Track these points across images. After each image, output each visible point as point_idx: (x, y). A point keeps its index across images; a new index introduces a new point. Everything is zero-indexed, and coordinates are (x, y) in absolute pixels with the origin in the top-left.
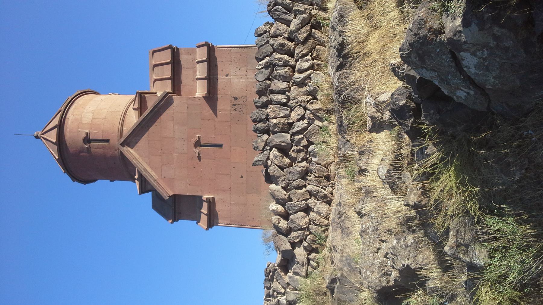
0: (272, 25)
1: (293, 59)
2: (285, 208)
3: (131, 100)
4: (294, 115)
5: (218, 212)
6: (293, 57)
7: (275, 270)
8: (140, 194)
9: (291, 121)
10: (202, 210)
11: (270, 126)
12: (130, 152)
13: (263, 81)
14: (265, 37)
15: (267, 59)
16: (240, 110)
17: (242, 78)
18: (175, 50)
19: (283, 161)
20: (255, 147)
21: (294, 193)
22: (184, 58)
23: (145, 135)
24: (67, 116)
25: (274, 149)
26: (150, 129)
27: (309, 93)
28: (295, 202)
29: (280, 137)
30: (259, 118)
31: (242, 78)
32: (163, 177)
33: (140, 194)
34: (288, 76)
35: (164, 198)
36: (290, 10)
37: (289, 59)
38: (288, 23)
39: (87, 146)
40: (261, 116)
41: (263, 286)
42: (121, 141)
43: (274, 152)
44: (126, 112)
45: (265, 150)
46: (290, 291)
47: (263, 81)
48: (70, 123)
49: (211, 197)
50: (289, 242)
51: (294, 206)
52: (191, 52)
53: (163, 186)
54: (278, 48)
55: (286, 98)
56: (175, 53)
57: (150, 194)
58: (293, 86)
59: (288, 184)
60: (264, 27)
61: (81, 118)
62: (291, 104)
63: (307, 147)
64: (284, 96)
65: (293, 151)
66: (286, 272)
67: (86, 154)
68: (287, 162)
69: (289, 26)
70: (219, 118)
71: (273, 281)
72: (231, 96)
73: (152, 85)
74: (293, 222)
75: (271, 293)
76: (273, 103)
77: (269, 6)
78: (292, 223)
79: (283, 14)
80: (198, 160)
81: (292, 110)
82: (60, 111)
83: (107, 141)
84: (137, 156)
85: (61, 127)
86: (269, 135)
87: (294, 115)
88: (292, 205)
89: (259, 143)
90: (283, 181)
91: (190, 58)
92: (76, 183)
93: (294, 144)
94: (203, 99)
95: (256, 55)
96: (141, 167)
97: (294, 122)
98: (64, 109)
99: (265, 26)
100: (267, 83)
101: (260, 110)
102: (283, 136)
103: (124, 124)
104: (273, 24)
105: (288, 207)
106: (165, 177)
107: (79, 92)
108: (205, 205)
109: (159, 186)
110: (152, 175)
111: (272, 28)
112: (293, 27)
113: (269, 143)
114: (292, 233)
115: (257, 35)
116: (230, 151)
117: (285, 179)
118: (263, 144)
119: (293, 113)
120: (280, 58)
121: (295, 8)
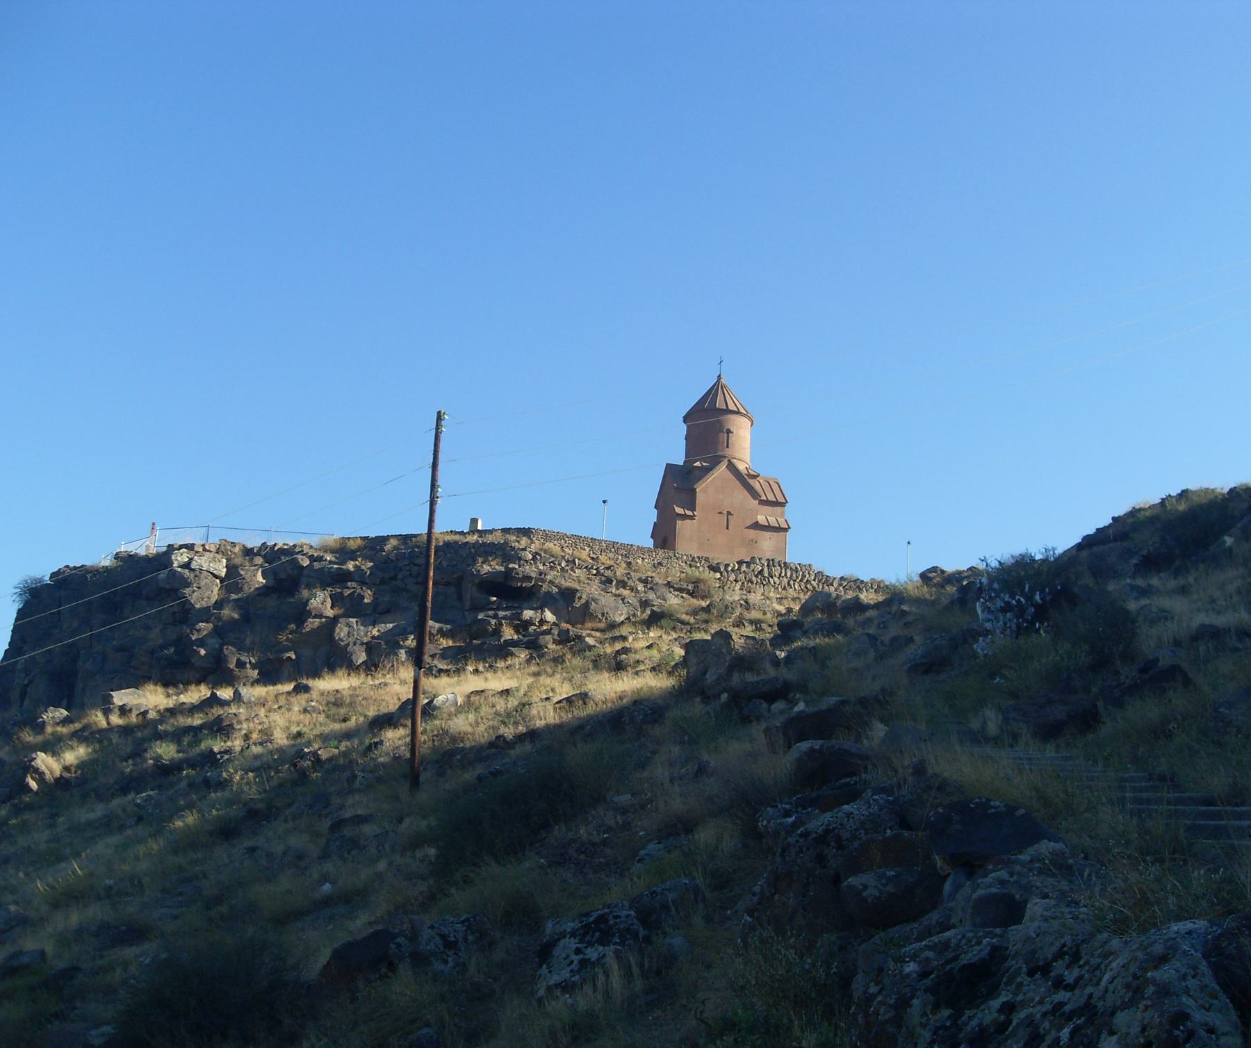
4: (776, 579)
6: (800, 581)
7: (709, 562)
22: (779, 508)
27: (785, 587)
36: (819, 582)
38: (814, 580)
39: (725, 430)
52: (782, 515)
56: (782, 505)
61: (741, 428)
63: (762, 583)
81: (779, 578)
83: (728, 447)
85: (738, 413)
108: (691, 514)
112: (813, 582)
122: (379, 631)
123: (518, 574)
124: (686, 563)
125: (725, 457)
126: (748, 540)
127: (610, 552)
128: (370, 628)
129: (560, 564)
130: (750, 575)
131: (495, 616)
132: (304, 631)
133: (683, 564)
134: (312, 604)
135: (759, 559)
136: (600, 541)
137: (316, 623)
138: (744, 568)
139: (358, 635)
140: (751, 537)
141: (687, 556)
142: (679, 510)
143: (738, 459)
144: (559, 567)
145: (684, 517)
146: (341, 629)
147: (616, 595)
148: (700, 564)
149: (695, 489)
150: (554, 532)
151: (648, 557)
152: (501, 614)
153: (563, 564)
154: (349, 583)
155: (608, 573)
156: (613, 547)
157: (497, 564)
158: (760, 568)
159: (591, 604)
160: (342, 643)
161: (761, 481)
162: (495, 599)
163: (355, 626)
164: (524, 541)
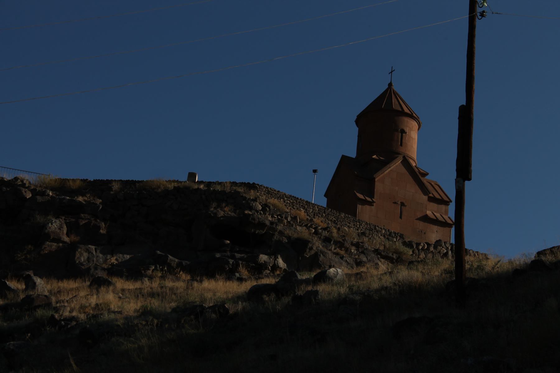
5: (365, 206)
7: (403, 239)
12: (399, 161)
13: (470, 253)
18: (448, 204)
22: (443, 207)
23: (408, 173)
24: (414, 121)
26: (411, 177)
39: (399, 130)
44: (414, 161)
48: (412, 122)
74: (422, 252)
82: (419, 118)
83: (401, 145)
85: (411, 116)
106: (385, 178)
118: (447, 246)
122: (116, 260)
123: (254, 219)
124: (384, 236)
125: (399, 154)
127: (322, 216)
128: (109, 256)
129: (286, 218)
131: (233, 257)
132: (42, 252)
133: (383, 237)
134: (50, 228)
135: (445, 243)
136: (314, 205)
137: (53, 247)
138: (432, 249)
139: (97, 261)
141: (385, 230)
142: (361, 196)
143: (410, 158)
144: (285, 221)
145: (365, 202)
146: (81, 254)
147: (334, 253)
148: (396, 240)
149: (374, 178)
150: (275, 191)
151: (353, 226)
152: (238, 255)
153: (289, 219)
154: (82, 215)
155: (325, 233)
156: (325, 212)
157: (229, 211)
158: (445, 251)
159: (320, 255)
160: (83, 267)
161: (425, 181)
162: (229, 242)
163: (94, 253)
164: (252, 194)
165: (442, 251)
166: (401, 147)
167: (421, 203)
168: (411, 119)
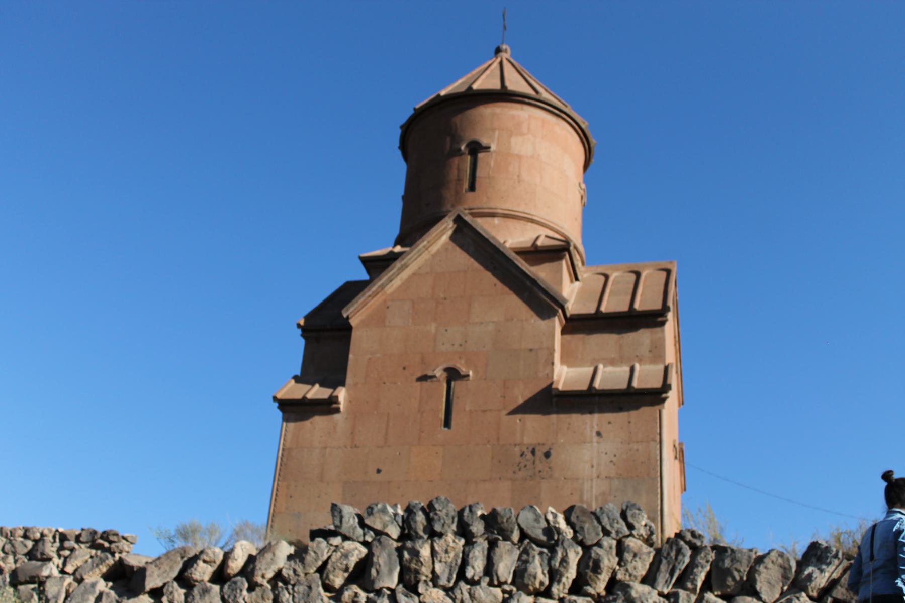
0: (648, 541)
1: (566, 591)
2: (236, 575)
3: (563, 231)
5: (311, 420)
7: (113, 554)
8: (360, 258)
9: (421, 588)
10: (317, 386)
11: (414, 542)
12: (442, 236)
13: (519, 525)
14: (619, 526)
15: (568, 532)
16: (522, 465)
17: (593, 467)
18: (660, 319)
19: (337, 571)
20: (372, 508)
21: (265, 597)
22: (644, 336)
23: (476, 265)
25: (364, 551)
26: (488, 275)
28: (244, 599)
29: (390, 563)
30: (436, 517)
31: (593, 467)
32: (389, 303)
33: (360, 258)
34: (526, 581)
35: (345, 309)
37: (566, 584)
38: (649, 579)
39: (463, 147)
40: (439, 520)
41: (86, 527)
42: (465, 215)
43: (357, 552)
45: (366, 530)
46: (66, 584)
47: (519, 525)
49: (342, 406)
50: (165, 585)
51: (235, 597)
53: (369, 304)
54: (590, 557)
55: (476, 578)
57: (365, 276)
58: (504, 592)
59: (286, 582)
60: (643, 523)
61: (522, 134)
62: (460, 589)
64: (480, 572)
65: (356, 595)
66: (106, 577)
67: (448, 147)
68: (334, 581)
69: (644, 581)
70: (506, 419)
71: (92, 547)
72: (553, 444)
73: (600, 270)
75: (67, 544)
76: (467, 549)
77: (693, 534)
78: (203, 590)
79: (671, 567)
80: (419, 375)
81: (448, 591)
83: (472, 188)
84: (435, 248)
85: (504, 96)
86: (398, 540)
87: (436, 597)
88: (238, 591)
89: (381, 518)
90: (295, 571)
91: (644, 351)
92: (398, 132)
93: (371, 595)
94: (549, 383)
95: (580, 507)
96: (411, 258)
97: (419, 595)
98: (542, 99)
99: (646, 525)
100: (512, 532)
101: (453, 518)
102: (391, 571)
103: (506, 219)
104: (651, 545)
105: (235, 583)
106: (388, 307)
107: (583, 126)
109: (370, 296)
110: (393, 282)
111: (640, 542)
113: (379, 541)
114: (183, 591)
115: (624, 507)
116: (434, 445)
117: (298, 576)
118: (378, 526)
119: (442, 593)
120: (567, 563)
121: (682, 594)
126: (517, 450)
130: (301, 589)
140: (529, 439)
143: (506, 216)
165: (336, 556)
166: (471, 194)
167: (531, 350)
168: (509, 104)
